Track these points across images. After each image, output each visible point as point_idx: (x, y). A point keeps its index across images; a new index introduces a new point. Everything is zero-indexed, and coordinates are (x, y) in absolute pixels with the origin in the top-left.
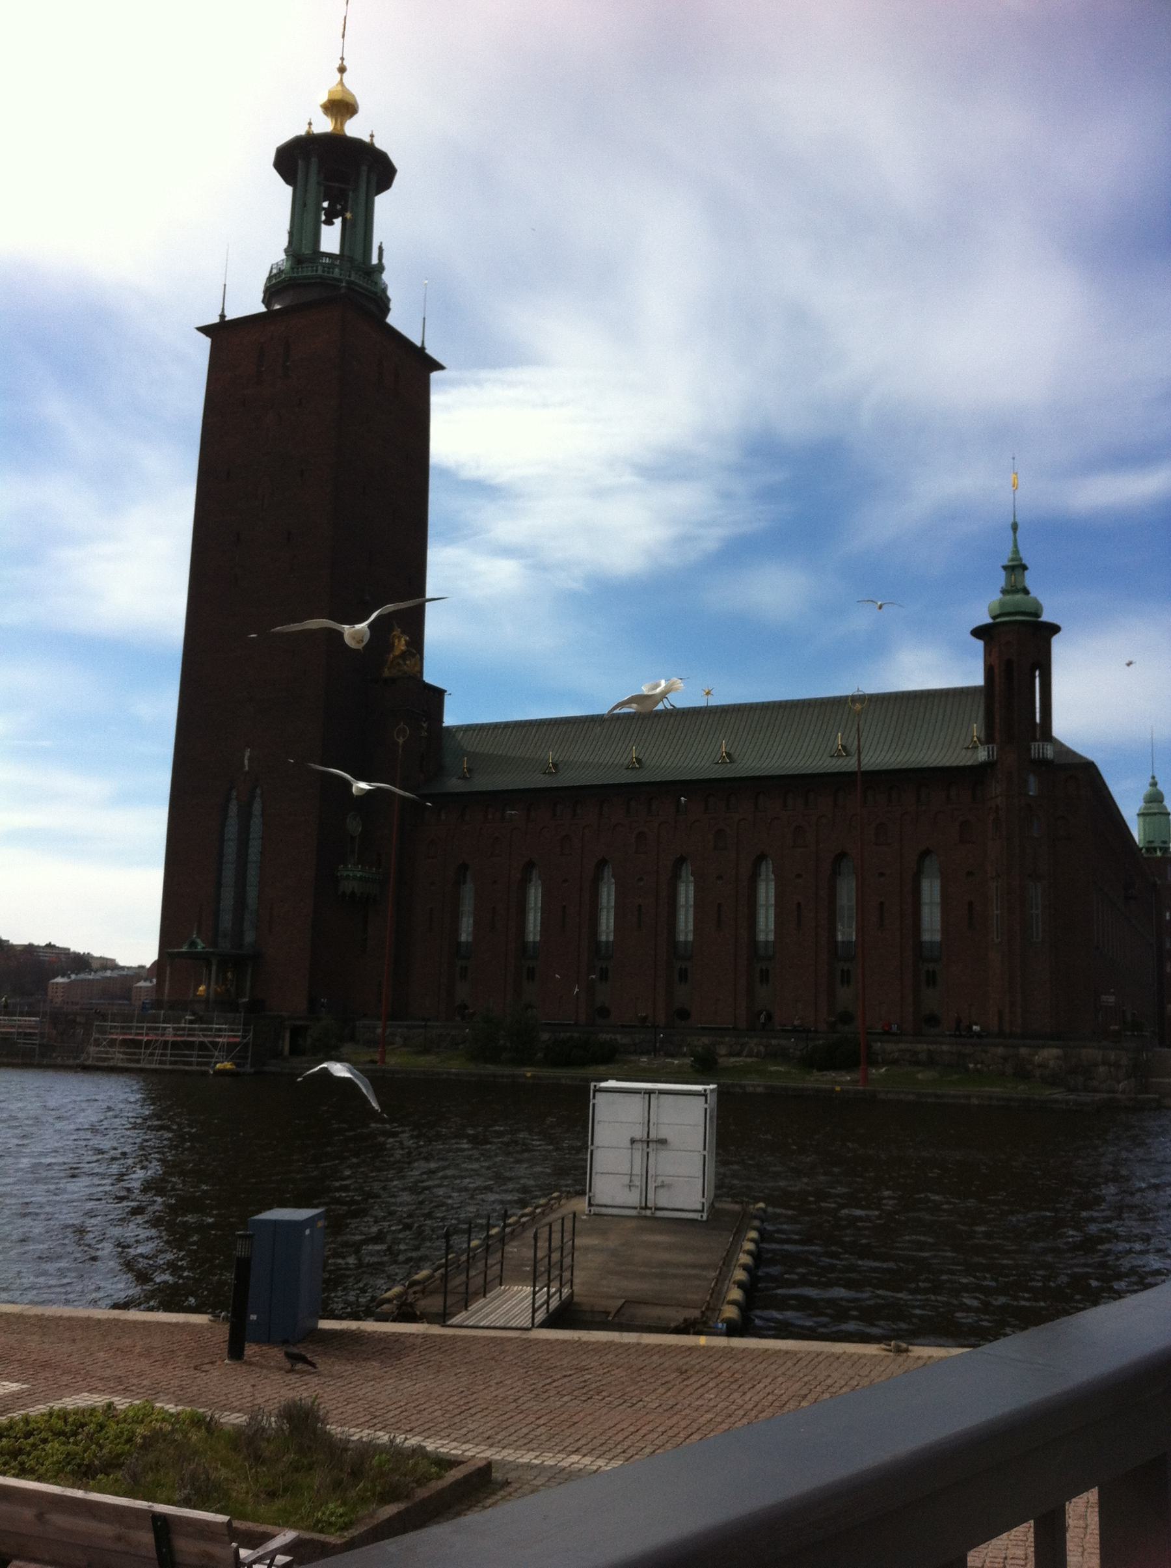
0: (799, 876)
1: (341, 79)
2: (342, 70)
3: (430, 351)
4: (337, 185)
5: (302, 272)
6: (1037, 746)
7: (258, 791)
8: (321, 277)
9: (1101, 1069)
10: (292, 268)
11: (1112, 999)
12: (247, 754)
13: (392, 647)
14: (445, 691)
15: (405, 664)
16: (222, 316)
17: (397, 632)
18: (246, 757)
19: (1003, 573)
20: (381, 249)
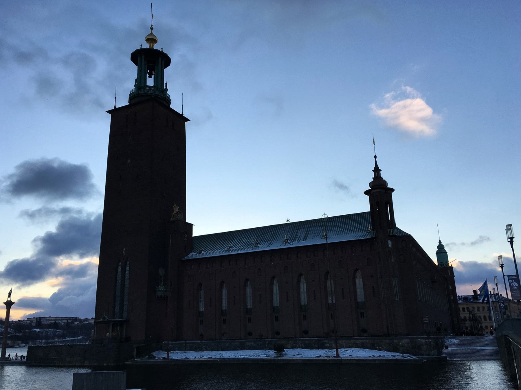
0: (313, 281)
1: (152, 32)
3: (185, 115)
4: (151, 64)
5: (140, 92)
6: (391, 230)
7: (128, 262)
8: (146, 93)
9: (424, 347)
10: (137, 91)
11: (427, 320)
12: (124, 250)
13: (173, 211)
14: (193, 224)
16: (115, 107)
17: (175, 205)
18: (124, 251)
20: (166, 84)
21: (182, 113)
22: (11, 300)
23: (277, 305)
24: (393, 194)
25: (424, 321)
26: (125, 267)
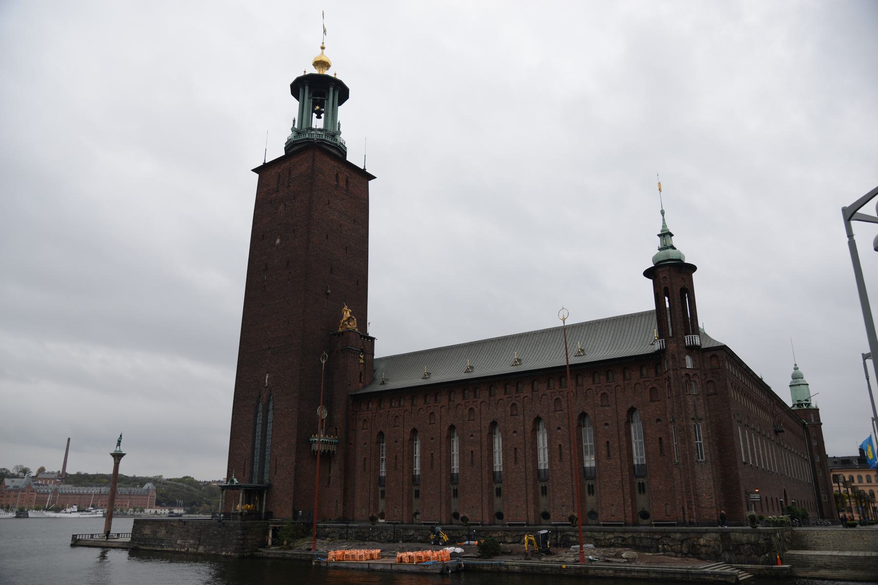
0: (559, 428)
1: (322, 52)
2: (323, 48)
4: (319, 98)
5: (299, 138)
8: (307, 139)
9: (746, 547)
10: (295, 137)
11: (757, 496)
12: (267, 377)
15: (349, 324)
17: (346, 308)
18: (266, 379)
19: (659, 238)
20: (339, 123)
21: (365, 166)
22: (122, 450)
23: (500, 468)
24: (695, 275)
25: (752, 498)
26: (268, 404)
